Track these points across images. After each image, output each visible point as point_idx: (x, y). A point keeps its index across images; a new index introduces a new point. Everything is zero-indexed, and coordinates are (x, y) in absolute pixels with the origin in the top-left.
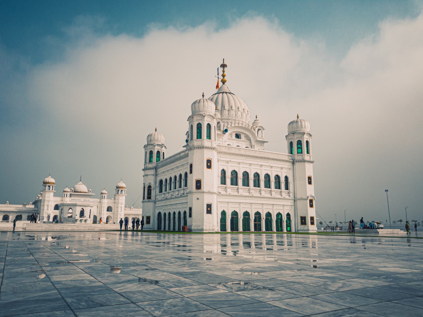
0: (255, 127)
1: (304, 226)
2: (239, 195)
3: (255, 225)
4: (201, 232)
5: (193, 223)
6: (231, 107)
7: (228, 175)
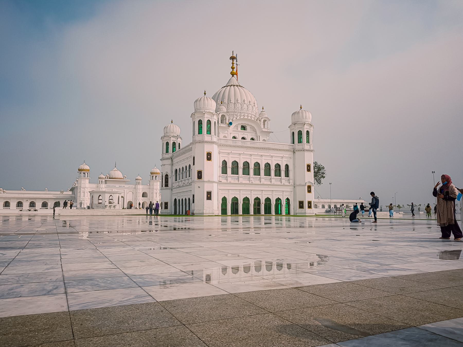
2: (240, 183)
3: (254, 209)
4: (202, 215)
5: (195, 207)
7: (229, 165)
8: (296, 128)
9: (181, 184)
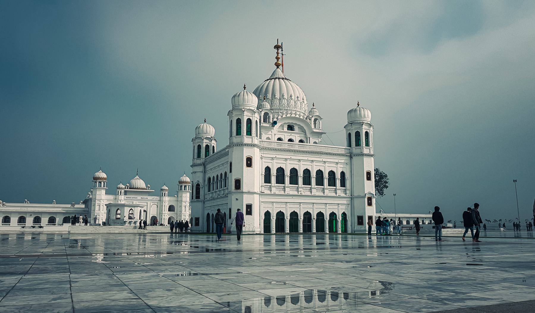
0: (311, 116)
1: (361, 226)
6: (283, 96)
7: (274, 172)
8: (353, 128)
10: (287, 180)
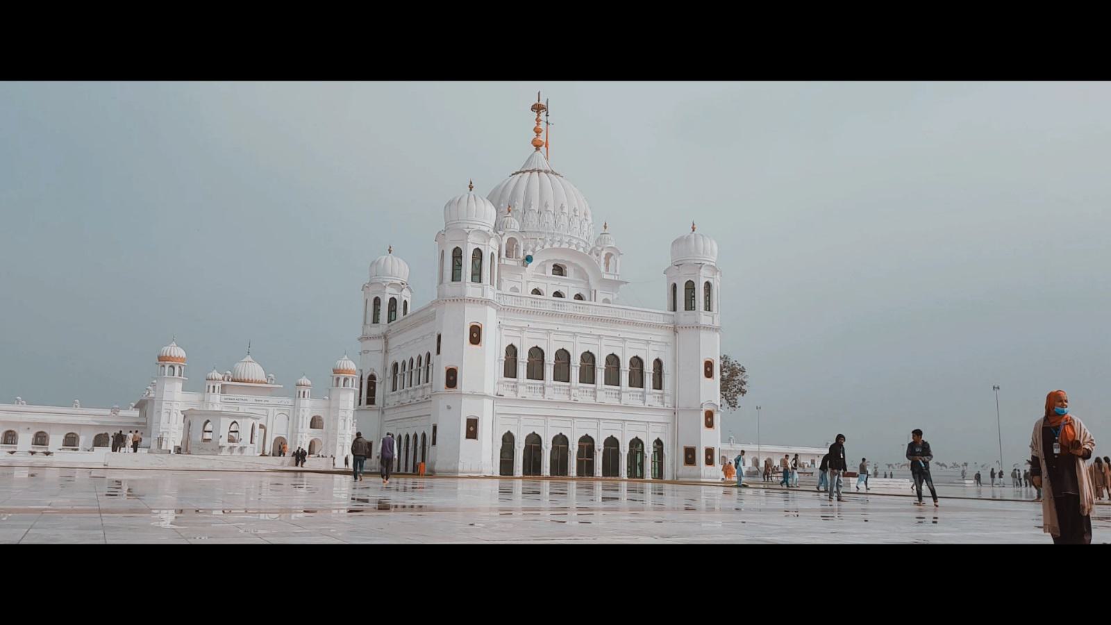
0: (599, 249)
3: (579, 463)
4: (452, 475)
5: (438, 456)
6: (546, 206)
7: (523, 357)
9: (405, 398)
10: (549, 371)
